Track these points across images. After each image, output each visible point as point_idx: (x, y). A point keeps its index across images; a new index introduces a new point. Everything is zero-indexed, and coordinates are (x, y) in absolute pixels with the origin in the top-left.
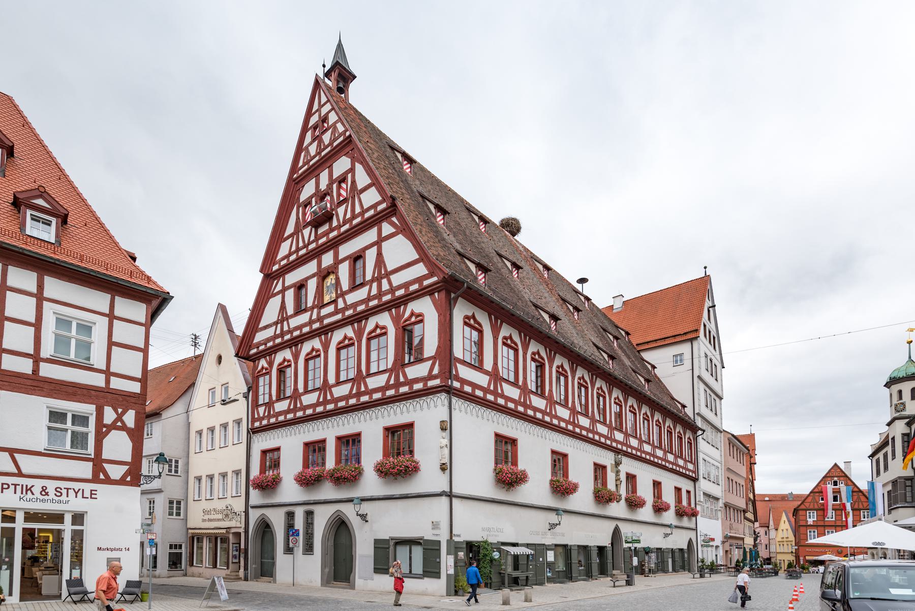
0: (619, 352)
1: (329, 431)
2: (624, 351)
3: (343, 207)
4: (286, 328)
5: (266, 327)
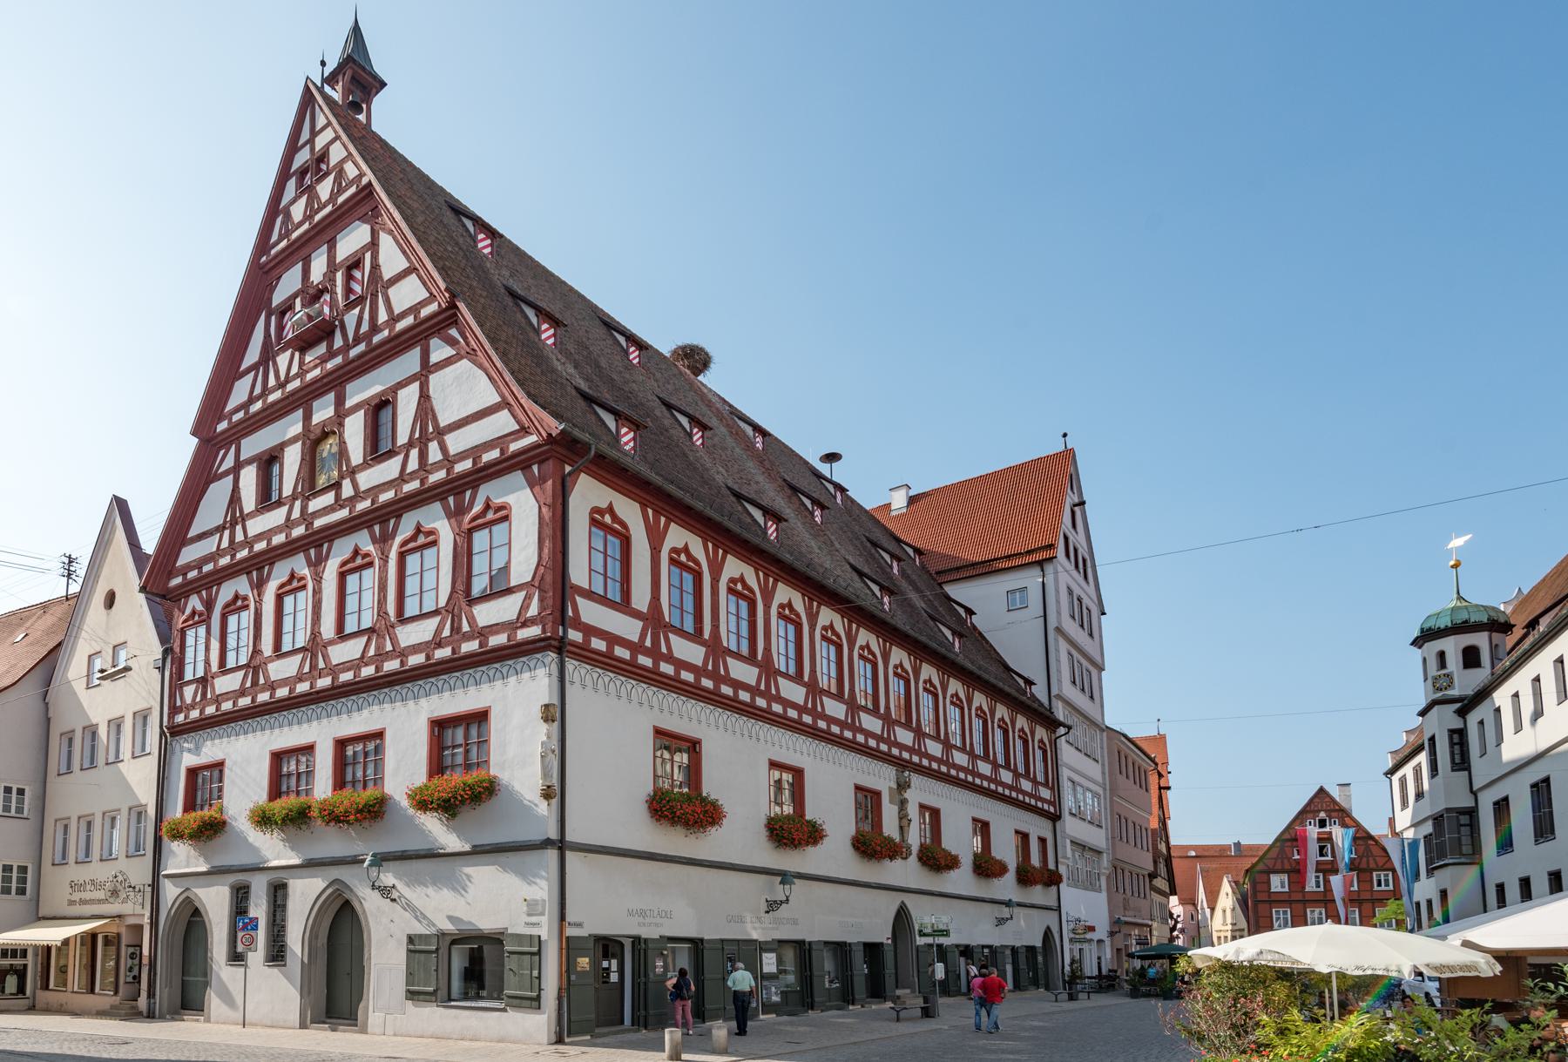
0: (904, 584)
1: (320, 732)
2: (912, 583)
4: (239, 537)
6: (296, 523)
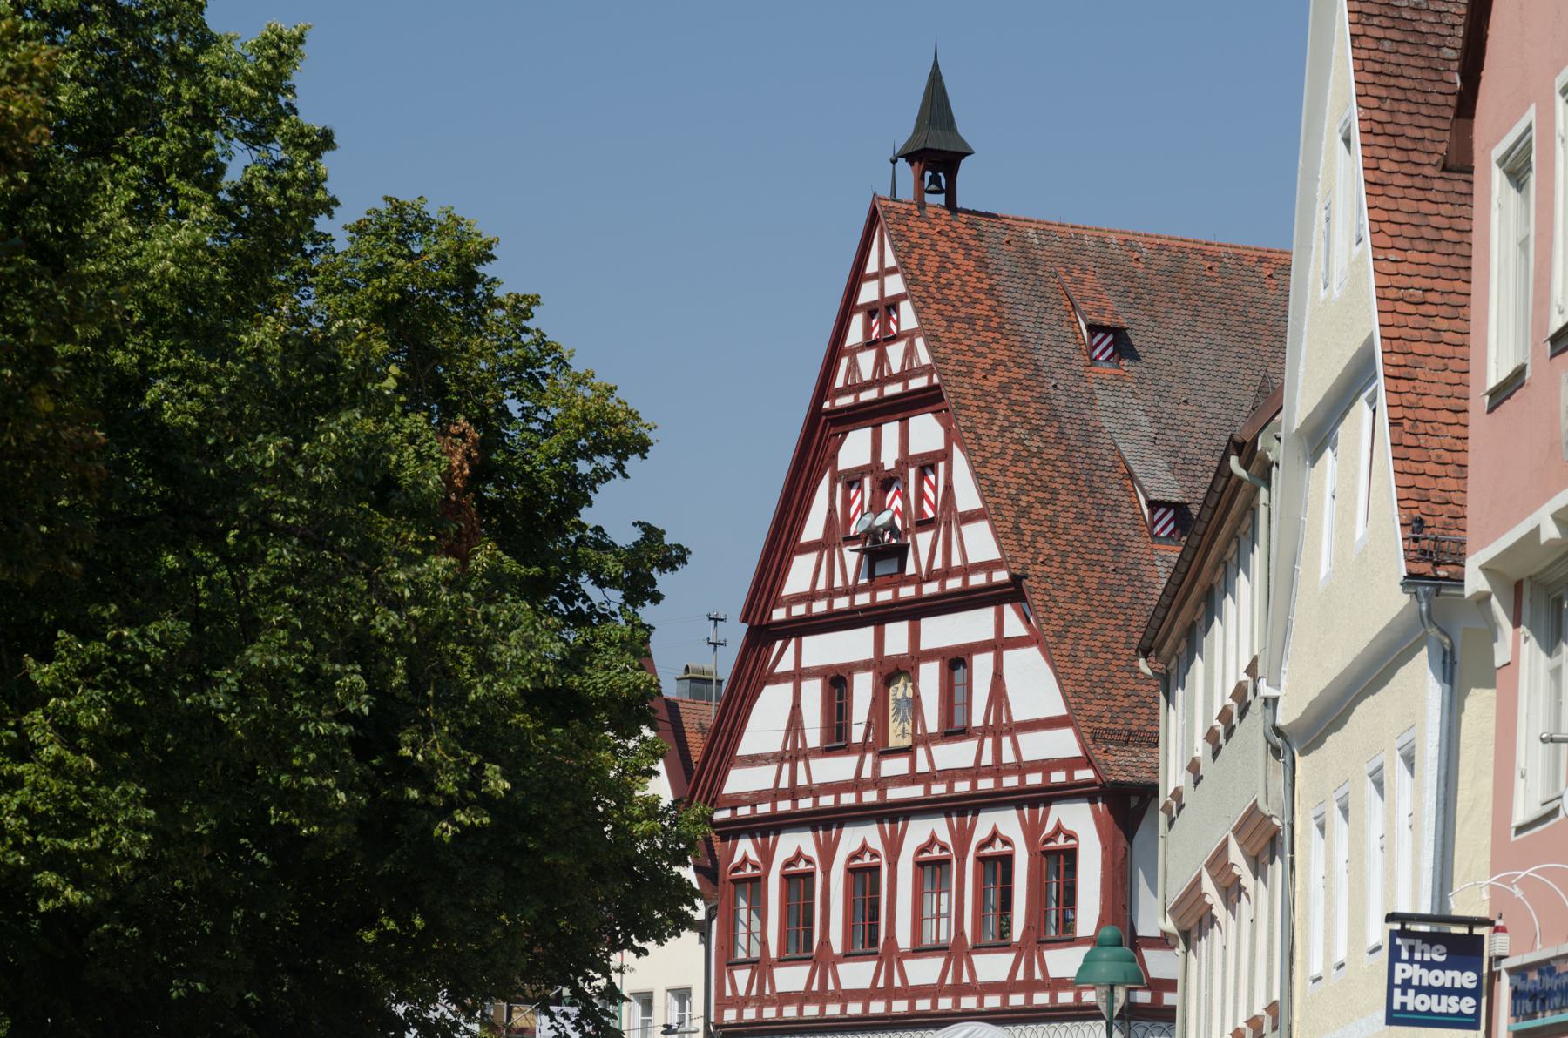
3: (929, 535)
5: (754, 760)
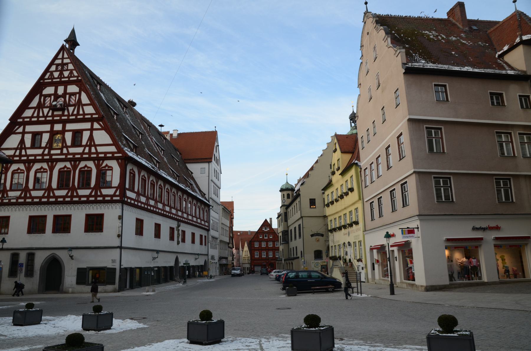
6: (46, 155)
